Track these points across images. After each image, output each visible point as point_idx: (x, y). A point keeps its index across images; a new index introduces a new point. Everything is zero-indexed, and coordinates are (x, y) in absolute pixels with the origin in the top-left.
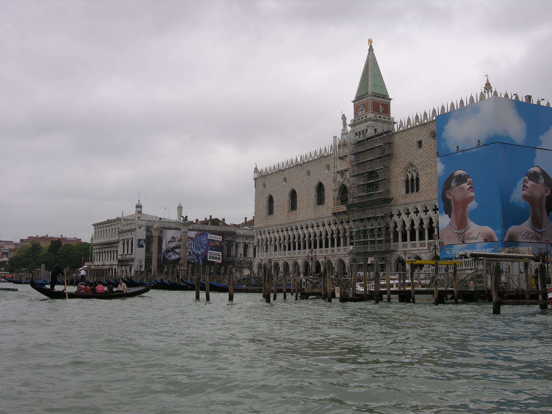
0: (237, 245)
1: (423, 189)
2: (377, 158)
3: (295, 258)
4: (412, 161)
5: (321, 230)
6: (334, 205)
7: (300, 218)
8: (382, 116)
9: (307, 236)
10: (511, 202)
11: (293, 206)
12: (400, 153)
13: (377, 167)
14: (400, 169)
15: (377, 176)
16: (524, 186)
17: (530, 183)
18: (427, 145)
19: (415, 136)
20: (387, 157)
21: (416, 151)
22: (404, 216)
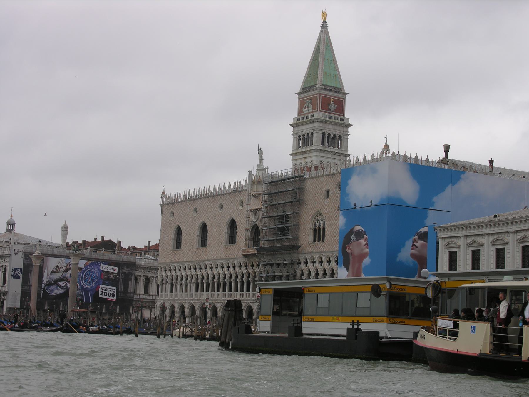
0: (136, 279)
1: (328, 239)
2: (287, 203)
5: (231, 272)
6: (245, 246)
10: (398, 260)
11: (203, 242)
13: (289, 212)
16: (413, 245)
17: (420, 243)
18: (334, 196)
19: (324, 185)
20: (298, 202)
21: (324, 200)
22: (310, 265)
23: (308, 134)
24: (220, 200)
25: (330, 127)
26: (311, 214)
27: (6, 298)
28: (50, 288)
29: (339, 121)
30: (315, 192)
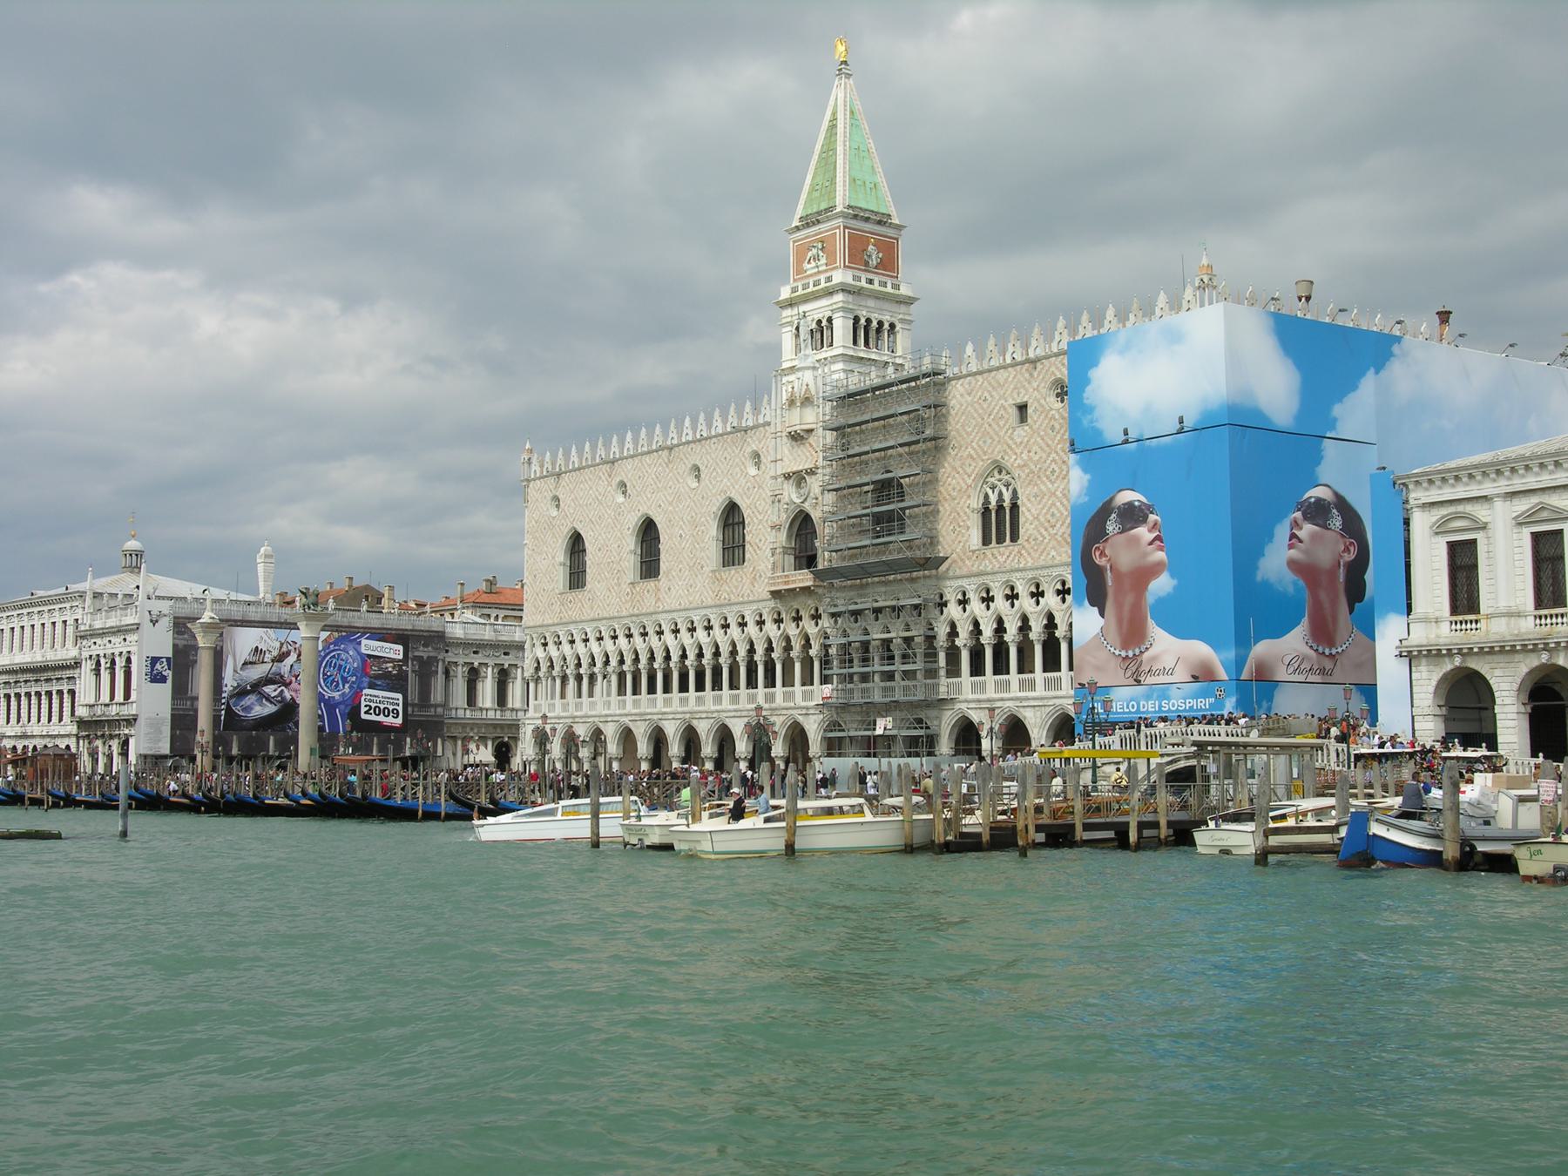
0: (447, 673)
3: (655, 717)
4: (999, 458)
7: (669, 602)
8: (876, 280)
9: (691, 655)
10: (1259, 578)
11: (650, 566)
12: (967, 433)
15: (902, 495)
16: (1293, 536)
17: (1307, 529)
21: (1010, 432)
25: (871, 303)
26: (974, 470)
27: (133, 732)
28: (243, 703)
29: (889, 289)
30: (981, 411)
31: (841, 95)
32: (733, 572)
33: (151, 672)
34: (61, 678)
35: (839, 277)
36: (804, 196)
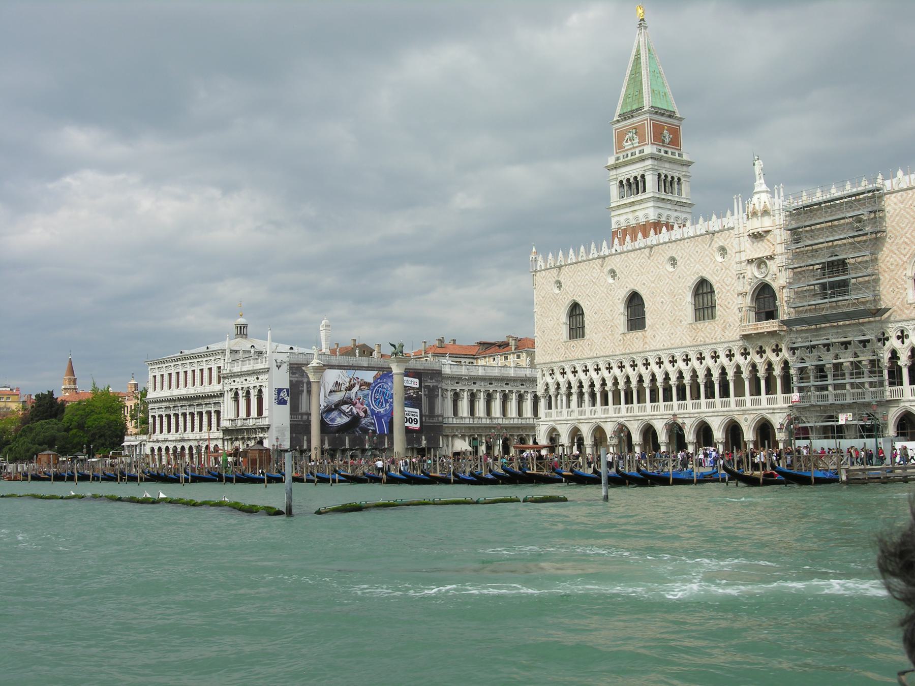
3: (647, 418)
7: (655, 344)
8: (670, 151)
14: (902, 256)
23: (635, 178)
24: (667, 251)
25: (667, 165)
26: (907, 253)
27: (266, 435)
28: (330, 416)
29: (677, 157)
31: (642, 40)
32: (707, 324)
33: (278, 398)
34: (210, 404)
35: (649, 149)
36: (620, 101)
